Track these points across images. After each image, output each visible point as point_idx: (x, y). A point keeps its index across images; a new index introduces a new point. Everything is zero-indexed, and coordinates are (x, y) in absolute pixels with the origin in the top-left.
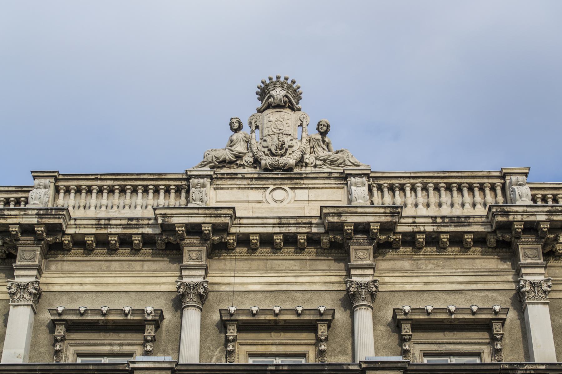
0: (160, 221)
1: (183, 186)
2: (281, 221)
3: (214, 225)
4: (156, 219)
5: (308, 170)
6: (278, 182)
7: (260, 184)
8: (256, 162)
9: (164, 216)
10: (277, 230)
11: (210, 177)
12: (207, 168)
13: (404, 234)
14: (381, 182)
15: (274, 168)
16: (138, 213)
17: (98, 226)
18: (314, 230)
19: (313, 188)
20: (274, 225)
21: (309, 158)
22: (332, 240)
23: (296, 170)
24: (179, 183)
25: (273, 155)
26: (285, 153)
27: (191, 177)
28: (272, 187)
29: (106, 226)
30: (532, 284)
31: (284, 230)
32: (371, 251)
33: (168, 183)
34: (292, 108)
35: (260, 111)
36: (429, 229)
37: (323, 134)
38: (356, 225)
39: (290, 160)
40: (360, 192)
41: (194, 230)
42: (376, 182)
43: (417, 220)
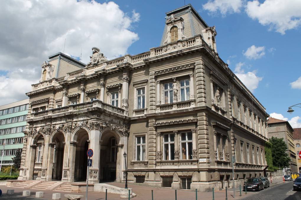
2: (92, 75)
5: (100, 63)
7: (93, 68)
15: (94, 64)
17: (72, 81)
20: (91, 76)
22: (97, 77)
29: (72, 81)
30: (124, 78)
36: (111, 71)
39: (96, 62)
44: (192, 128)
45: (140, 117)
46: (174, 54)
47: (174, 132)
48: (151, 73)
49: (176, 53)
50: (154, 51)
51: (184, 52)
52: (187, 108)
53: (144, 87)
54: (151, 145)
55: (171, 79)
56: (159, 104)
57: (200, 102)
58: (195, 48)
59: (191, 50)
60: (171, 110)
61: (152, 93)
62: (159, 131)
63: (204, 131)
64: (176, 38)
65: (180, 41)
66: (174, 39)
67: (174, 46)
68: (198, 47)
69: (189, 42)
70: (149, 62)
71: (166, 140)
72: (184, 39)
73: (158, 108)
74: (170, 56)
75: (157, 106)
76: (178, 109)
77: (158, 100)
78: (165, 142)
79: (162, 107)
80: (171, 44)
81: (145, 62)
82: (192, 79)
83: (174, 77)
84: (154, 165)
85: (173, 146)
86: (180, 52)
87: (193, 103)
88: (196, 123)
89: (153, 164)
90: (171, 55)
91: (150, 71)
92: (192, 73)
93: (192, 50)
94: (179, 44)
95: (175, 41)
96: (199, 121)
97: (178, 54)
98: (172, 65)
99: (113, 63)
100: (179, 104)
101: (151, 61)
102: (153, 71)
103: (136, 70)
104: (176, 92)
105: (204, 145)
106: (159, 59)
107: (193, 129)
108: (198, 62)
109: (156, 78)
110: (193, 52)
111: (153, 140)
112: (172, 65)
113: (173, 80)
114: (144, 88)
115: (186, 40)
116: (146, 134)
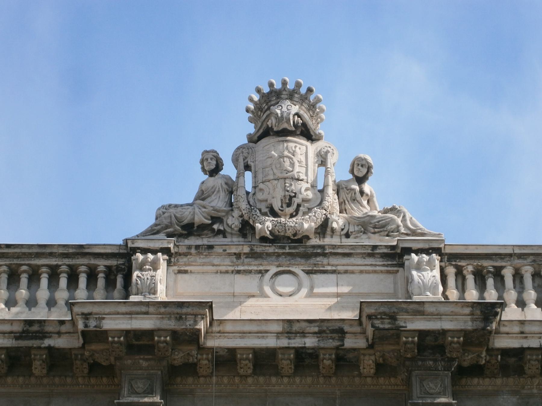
0: (81, 326)
1: (117, 267)
2: (290, 327)
3: (174, 333)
4: (73, 322)
6: (282, 260)
8: (246, 228)
9: (86, 316)
10: (284, 342)
11: (166, 251)
12: (162, 236)
13: (506, 352)
14: (462, 263)
15: (275, 239)
16: (40, 313)
18: (349, 343)
19: (346, 272)
20: (278, 335)
21: (338, 221)
23: (315, 241)
24: (113, 262)
25: (274, 213)
26: (297, 211)
27: (134, 250)
28: (273, 270)
31: (297, 342)
32: (448, 381)
33: (93, 261)
34: (307, 134)
35: (254, 140)
37: (361, 180)
38: (422, 334)
40: (427, 276)
41: (138, 343)
42: (454, 260)
43: (527, 328)
99: (518, 276)
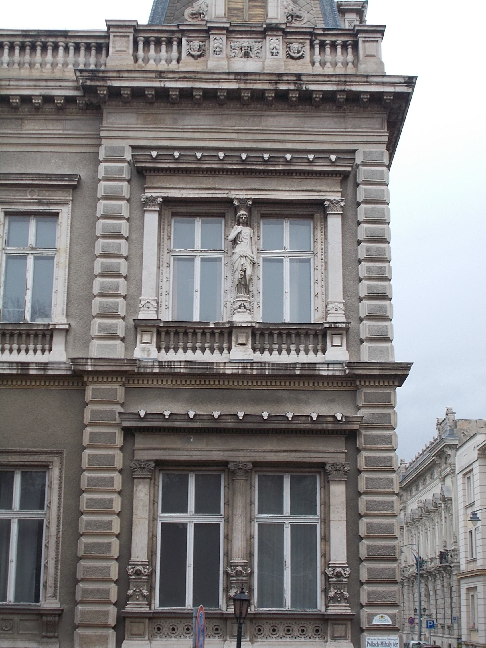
44: (331, 453)
45: (28, 363)
46: (255, 81)
47: (231, 466)
48: (113, 149)
49: (270, 82)
50: (131, 38)
51: (312, 87)
52: (311, 358)
53: (53, 208)
54: (100, 524)
55: (229, 202)
56: (152, 316)
57: (372, 339)
58: (370, 83)
59: (348, 88)
60: (225, 356)
61: (112, 250)
62: (149, 450)
63: (391, 481)
64: (250, 7)
65: (283, 30)
66: (241, 10)
67: (245, 42)
68: (383, 84)
69: (322, 45)
70: (110, 88)
71: (174, 502)
72: (297, 24)
73: (146, 338)
74: (234, 86)
75: (141, 326)
76: (258, 357)
77: (148, 292)
78: (165, 510)
79: (170, 333)
80: (230, 32)
81: (88, 83)
82: (334, 223)
83: (242, 195)
84: (111, 634)
85: (207, 534)
86: (289, 82)
87: (337, 341)
88: (351, 436)
89: (106, 626)
90: (242, 86)
91: (102, 134)
92: (337, 197)
93: (355, 88)
94: (275, 42)
95: (255, 17)
96: (366, 428)
97: (277, 91)
98: (234, 136)
100: (265, 334)
101: (119, 88)
102: (124, 134)
103: (16, 108)
104: (249, 272)
105: (387, 547)
106: (169, 85)
107: (333, 465)
108: (370, 153)
109: (142, 174)
110: (354, 98)
111: (111, 501)
112: (234, 136)
113: (236, 209)
114: (56, 215)
115: (310, 34)
116: (56, 459)
